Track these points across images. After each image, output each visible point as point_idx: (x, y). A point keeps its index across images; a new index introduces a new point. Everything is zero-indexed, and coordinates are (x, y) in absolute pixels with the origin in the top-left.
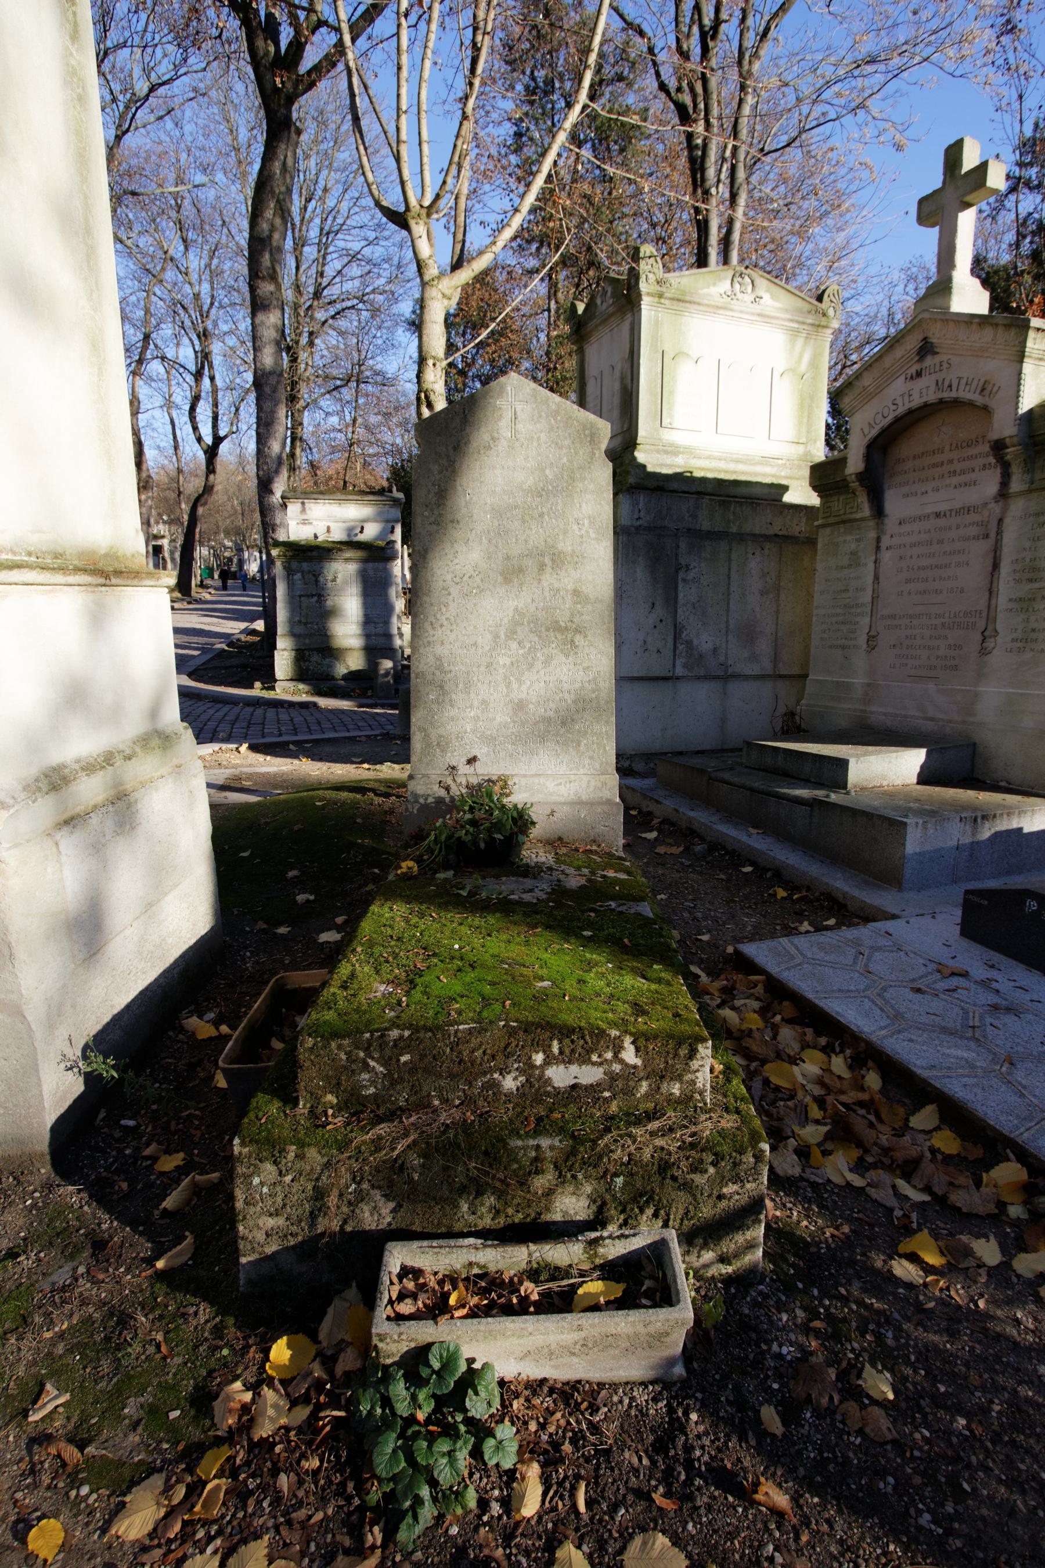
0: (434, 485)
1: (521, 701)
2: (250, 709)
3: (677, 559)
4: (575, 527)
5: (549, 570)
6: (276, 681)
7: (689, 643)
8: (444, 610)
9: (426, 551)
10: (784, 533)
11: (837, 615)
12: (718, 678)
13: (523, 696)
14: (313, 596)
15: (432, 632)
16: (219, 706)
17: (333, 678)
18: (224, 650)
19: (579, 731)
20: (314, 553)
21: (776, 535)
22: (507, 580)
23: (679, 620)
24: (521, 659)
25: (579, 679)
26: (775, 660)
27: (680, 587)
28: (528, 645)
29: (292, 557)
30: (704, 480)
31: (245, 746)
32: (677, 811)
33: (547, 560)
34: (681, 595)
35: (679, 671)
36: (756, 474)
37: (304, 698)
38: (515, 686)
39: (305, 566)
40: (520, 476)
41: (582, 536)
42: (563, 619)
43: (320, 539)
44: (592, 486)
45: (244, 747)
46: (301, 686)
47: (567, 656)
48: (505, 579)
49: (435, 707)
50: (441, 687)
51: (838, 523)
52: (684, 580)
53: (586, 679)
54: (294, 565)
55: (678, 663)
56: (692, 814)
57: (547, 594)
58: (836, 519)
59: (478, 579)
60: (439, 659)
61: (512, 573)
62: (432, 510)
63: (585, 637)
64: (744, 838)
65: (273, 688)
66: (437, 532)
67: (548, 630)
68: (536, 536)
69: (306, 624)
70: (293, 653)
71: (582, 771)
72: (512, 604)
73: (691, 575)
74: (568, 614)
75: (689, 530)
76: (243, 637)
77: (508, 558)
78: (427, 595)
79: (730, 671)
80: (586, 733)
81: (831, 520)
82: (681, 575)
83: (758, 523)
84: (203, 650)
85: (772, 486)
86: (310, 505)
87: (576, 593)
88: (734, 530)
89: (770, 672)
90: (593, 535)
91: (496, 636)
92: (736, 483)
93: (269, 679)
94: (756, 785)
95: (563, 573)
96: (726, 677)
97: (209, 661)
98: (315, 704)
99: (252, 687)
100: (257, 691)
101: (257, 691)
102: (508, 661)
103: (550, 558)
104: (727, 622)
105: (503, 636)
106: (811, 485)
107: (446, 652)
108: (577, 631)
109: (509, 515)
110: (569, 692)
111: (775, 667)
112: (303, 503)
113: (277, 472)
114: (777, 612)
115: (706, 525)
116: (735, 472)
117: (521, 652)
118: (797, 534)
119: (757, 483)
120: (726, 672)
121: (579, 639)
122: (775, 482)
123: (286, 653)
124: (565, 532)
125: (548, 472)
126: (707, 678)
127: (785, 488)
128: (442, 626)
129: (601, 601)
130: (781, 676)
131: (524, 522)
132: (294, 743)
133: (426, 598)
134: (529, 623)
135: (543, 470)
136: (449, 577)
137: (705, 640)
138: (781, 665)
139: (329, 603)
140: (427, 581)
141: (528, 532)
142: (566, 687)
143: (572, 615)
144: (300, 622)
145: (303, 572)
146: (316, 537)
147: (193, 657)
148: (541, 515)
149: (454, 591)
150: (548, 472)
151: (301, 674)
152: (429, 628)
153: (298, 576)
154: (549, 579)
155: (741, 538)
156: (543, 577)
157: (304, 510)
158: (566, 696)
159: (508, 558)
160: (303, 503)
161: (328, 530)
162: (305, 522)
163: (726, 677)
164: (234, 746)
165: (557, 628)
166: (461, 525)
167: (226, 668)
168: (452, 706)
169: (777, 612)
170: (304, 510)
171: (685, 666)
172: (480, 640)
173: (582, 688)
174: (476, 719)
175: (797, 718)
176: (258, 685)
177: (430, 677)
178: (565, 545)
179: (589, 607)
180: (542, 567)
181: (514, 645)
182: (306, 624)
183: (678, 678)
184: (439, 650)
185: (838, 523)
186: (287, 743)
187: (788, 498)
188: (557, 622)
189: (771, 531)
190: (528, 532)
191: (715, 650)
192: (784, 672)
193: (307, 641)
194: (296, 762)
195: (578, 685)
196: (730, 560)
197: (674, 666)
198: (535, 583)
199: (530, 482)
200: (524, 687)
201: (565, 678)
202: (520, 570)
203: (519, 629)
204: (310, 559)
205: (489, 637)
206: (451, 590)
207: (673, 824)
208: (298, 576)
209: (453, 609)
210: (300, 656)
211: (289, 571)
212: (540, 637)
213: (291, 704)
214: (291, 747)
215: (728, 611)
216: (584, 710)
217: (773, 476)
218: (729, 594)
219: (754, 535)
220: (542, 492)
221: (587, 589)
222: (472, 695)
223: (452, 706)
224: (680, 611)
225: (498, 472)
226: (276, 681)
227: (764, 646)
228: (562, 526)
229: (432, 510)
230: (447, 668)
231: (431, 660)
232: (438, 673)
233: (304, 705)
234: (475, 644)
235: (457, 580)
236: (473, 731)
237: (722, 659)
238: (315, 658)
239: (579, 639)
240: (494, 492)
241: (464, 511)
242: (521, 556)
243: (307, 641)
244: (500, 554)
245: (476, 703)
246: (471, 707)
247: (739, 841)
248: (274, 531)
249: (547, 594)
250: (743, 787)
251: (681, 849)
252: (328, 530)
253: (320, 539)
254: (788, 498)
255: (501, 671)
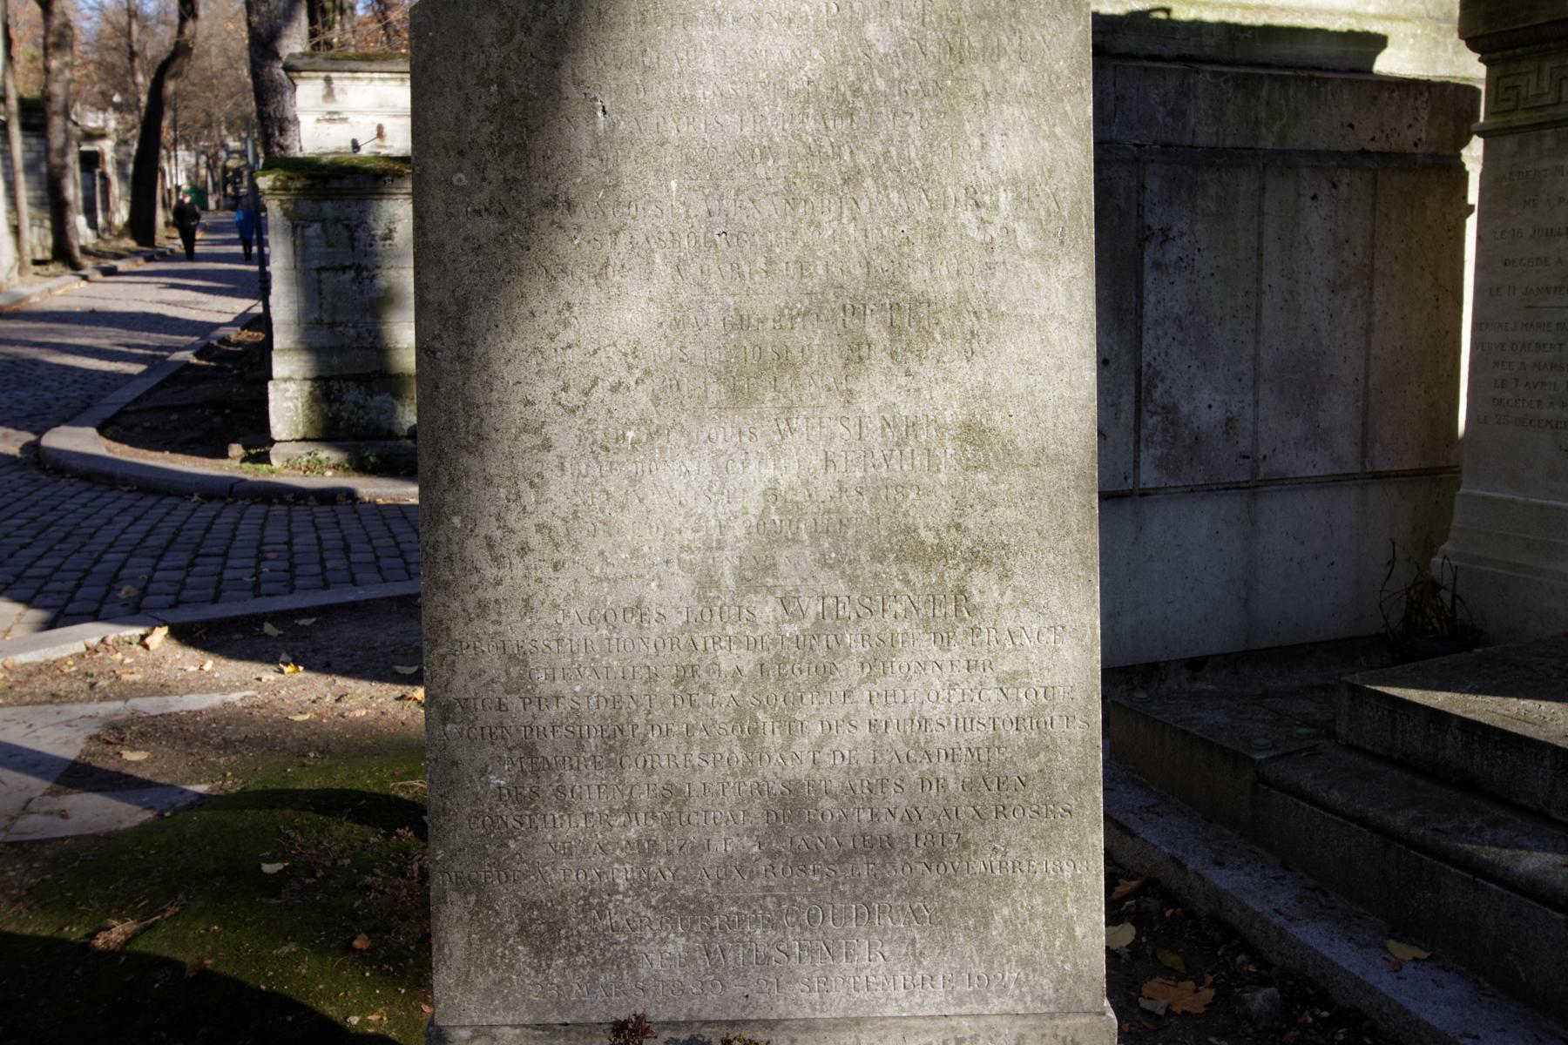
0: (483, 82)
1: (794, 787)
2: (210, 509)
3: (1140, 216)
4: (967, 216)
5: (879, 359)
6: (272, 442)
7: (1169, 410)
8: (529, 497)
9: (464, 306)
10: (1381, 145)
11: (1539, 346)
12: (1238, 487)
13: (801, 771)
14: (344, 269)
15: (491, 573)
16: (149, 501)
17: (391, 435)
18: (188, 365)
19: (986, 880)
20: (347, 183)
21: (1363, 152)
22: (739, 396)
23: (1147, 358)
24: (793, 653)
25: (985, 713)
26: (1364, 442)
27: (1148, 283)
28: (814, 608)
29: (303, 193)
30: (1196, 28)
31: (160, 633)
32: (1181, 866)
33: (874, 328)
34: (1151, 300)
35: (1149, 476)
36: (1313, 12)
37: (330, 480)
38: (773, 739)
39: (328, 208)
40: (777, 47)
41: (989, 247)
42: (928, 516)
43: (365, 151)
44: (1022, 78)
45: (160, 633)
46: (326, 454)
47: (944, 641)
48: (734, 391)
49: (509, 813)
50: (529, 750)
51: (1539, 126)
52: (1157, 265)
53: (1008, 712)
54: (307, 207)
55: (1146, 456)
56: (1223, 879)
57: (874, 440)
58: (1536, 117)
59: (642, 396)
60: (517, 657)
61: (752, 372)
62: (479, 167)
63: (1005, 576)
64: (1384, 982)
65: (264, 458)
66: (500, 240)
67: (879, 556)
68: (839, 238)
69: (332, 326)
70: (307, 386)
71: (996, 1004)
72: (757, 474)
73: (1173, 253)
74: (947, 507)
75: (1166, 145)
76: (234, 334)
77: (741, 323)
78: (470, 449)
79: (1264, 470)
80: (1009, 884)
81: (1520, 118)
82: (1150, 254)
83: (1326, 125)
84: (154, 362)
85: (1351, 36)
86: (341, 82)
87: (973, 433)
88: (1269, 143)
89: (1352, 466)
90: (1027, 242)
91: (707, 582)
92: (1269, 33)
93: (259, 441)
94: (1399, 821)
95: (927, 370)
96: (1254, 485)
97: (150, 392)
98: (350, 494)
99: (225, 456)
100: (232, 465)
101: (232, 465)
102: (748, 661)
103: (884, 315)
104: (1256, 358)
105: (729, 581)
106: (1461, 36)
107: (542, 636)
108: (978, 557)
109: (741, 178)
110: (951, 756)
111: (1364, 454)
112: (328, 80)
113: (289, 16)
114: (1369, 330)
115: (1205, 135)
116: (1265, 8)
117: (790, 629)
118: (1409, 148)
119: (1317, 31)
120: (1254, 474)
121: (982, 584)
122: (1357, 27)
123: (292, 387)
124: (935, 234)
125: (871, 30)
126: (1210, 489)
127: (1377, 42)
128: (524, 550)
129: (1056, 460)
130: (1378, 476)
131: (793, 201)
132: (278, 617)
133: (465, 460)
134: (815, 536)
135: (855, 25)
136: (543, 390)
137: (1205, 405)
138: (1377, 450)
139: (382, 282)
140: (470, 405)
141: (807, 235)
142: (942, 738)
143: (960, 505)
144: (319, 322)
145: (323, 221)
146: (356, 146)
147: (129, 377)
148: (852, 178)
149: (564, 434)
150: (871, 30)
151: (329, 426)
152: (482, 559)
153: (315, 229)
154: (879, 390)
155: (1286, 161)
156: (860, 385)
157: (329, 94)
158: (944, 767)
159: (741, 323)
160: (328, 80)
161: (380, 133)
162: (333, 117)
163: (1254, 485)
164: (140, 631)
165: (910, 550)
166: (580, 217)
167: (176, 408)
168: (565, 808)
169: (1369, 330)
170: (329, 94)
171: (1161, 464)
172: (652, 593)
173: (995, 743)
174: (646, 849)
175: (1446, 596)
176: (236, 450)
177: (489, 718)
178: (933, 278)
179: (1017, 480)
180: (856, 353)
181: (767, 610)
182: (332, 326)
183: (1144, 494)
184: (516, 629)
185: (1539, 126)
186: (259, 619)
187: (1387, 64)
188: (910, 530)
189: (1353, 143)
190: (807, 235)
191: (1229, 424)
192: (1384, 466)
193: (335, 361)
194: (269, 675)
195: (979, 734)
196: (1261, 213)
197: (1136, 463)
198: (836, 405)
199: (814, 65)
200: (802, 745)
201: (936, 712)
202: (784, 362)
203: (783, 556)
204: (337, 195)
205: (683, 583)
206: (552, 431)
207: (1170, 898)
208: (315, 229)
209: (560, 492)
210: (325, 389)
211: (297, 223)
212: (852, 580)
213: (300, 496)
214: (268, 628)
215: (1257, 332)
216: (1001, 810)
217: (1351, 14)
218: (1259, 294)
219: (1316, 154)
220: (845, 102)
221: (1011, 423)
222: (632, 774)
223: (565, 808)
224: (1148, 338)
225: (701, 34)
226: (272, 442)
227: (1339, 410)
228: (921, 213)
229: (479, 167)
230: (545, 689)
231: (492, 663)
232: (515, 702)
233: (327, 496)
234: (637, 608)
235: (573, 397)
236: (637, 887)
237: (1245, 444)
238: (353, 394)
239: (982, 584)
240: (690, 102)
241: (590, 167)
242: (789, 316)
243: (335, 361)
244: (713, 310)
245: (644, 798)
246: (630, 809)
247: (1371, 990)
248: (283, 131)
249: (874, 440)
250: (1362, 821)
251: (1208, 994)
252: (380, 133)
253: (365, 151)
254: (1387, 64)
255: (724, 694)
